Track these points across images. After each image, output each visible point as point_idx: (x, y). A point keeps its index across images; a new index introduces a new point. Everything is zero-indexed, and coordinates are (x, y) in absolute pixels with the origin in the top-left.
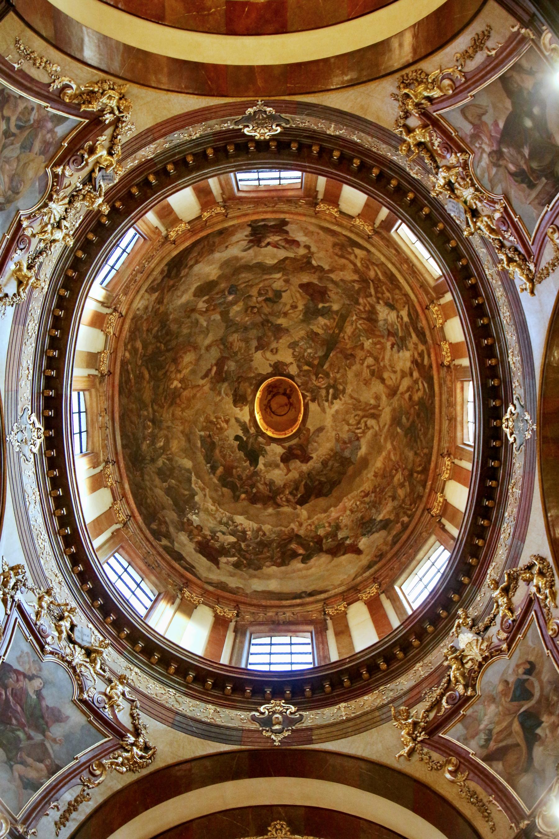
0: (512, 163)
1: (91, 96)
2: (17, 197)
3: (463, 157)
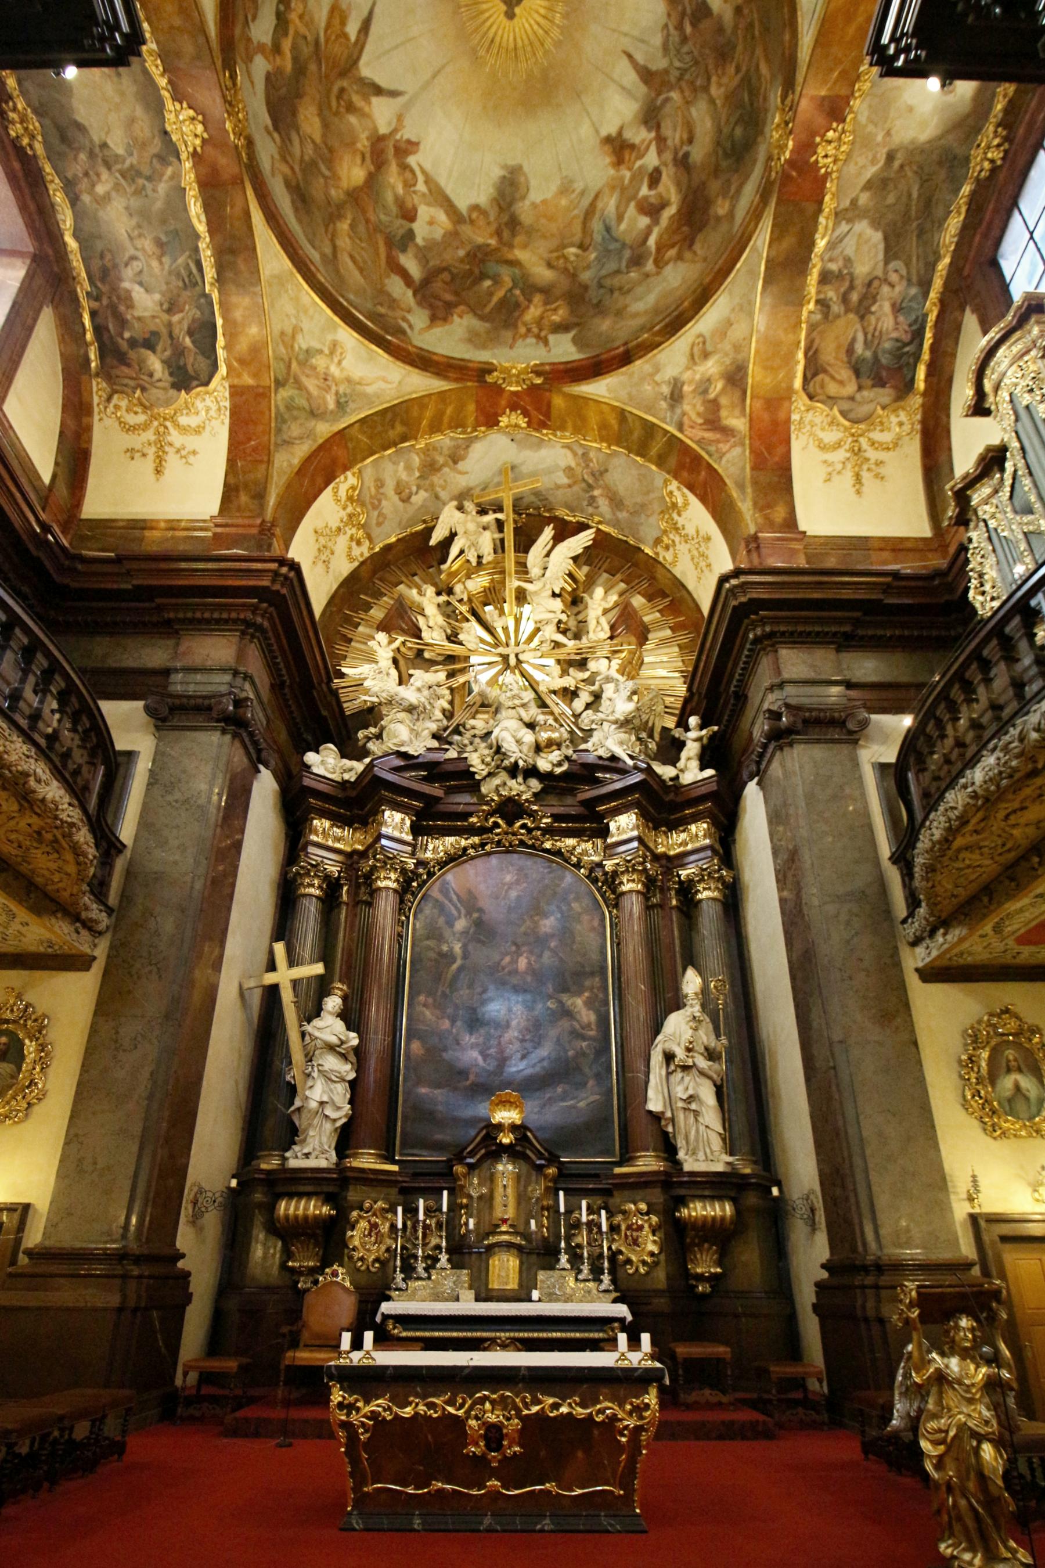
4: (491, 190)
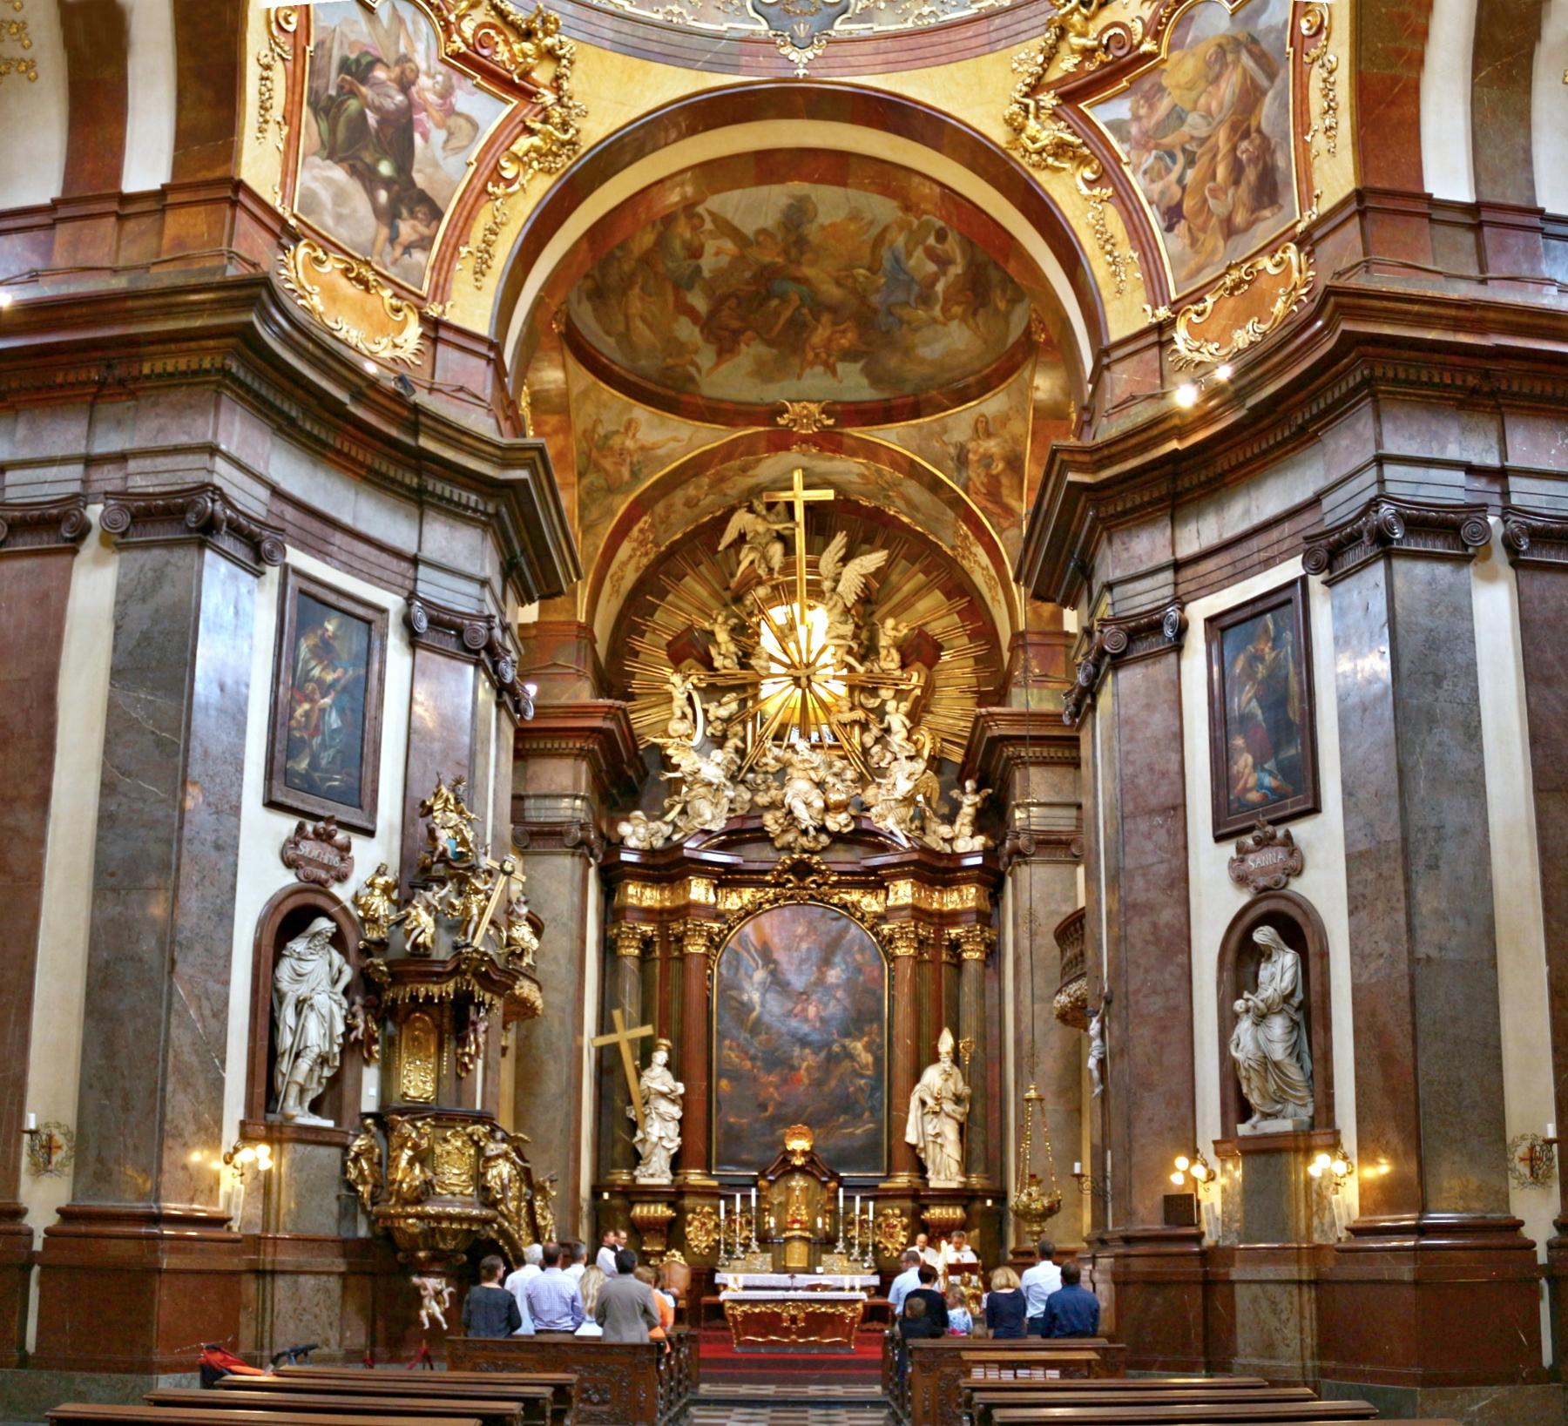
0: (382, 83)
1: (1061, 149)
2: (1223, 41)
3: (454, 46)
4: (778, 216)
